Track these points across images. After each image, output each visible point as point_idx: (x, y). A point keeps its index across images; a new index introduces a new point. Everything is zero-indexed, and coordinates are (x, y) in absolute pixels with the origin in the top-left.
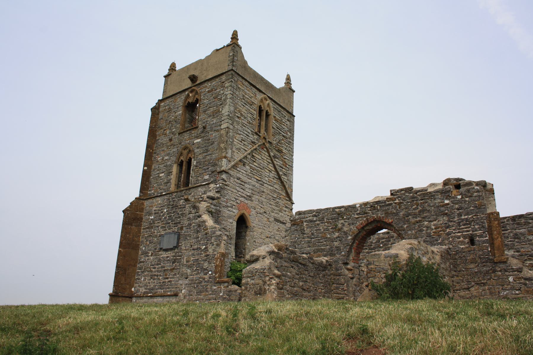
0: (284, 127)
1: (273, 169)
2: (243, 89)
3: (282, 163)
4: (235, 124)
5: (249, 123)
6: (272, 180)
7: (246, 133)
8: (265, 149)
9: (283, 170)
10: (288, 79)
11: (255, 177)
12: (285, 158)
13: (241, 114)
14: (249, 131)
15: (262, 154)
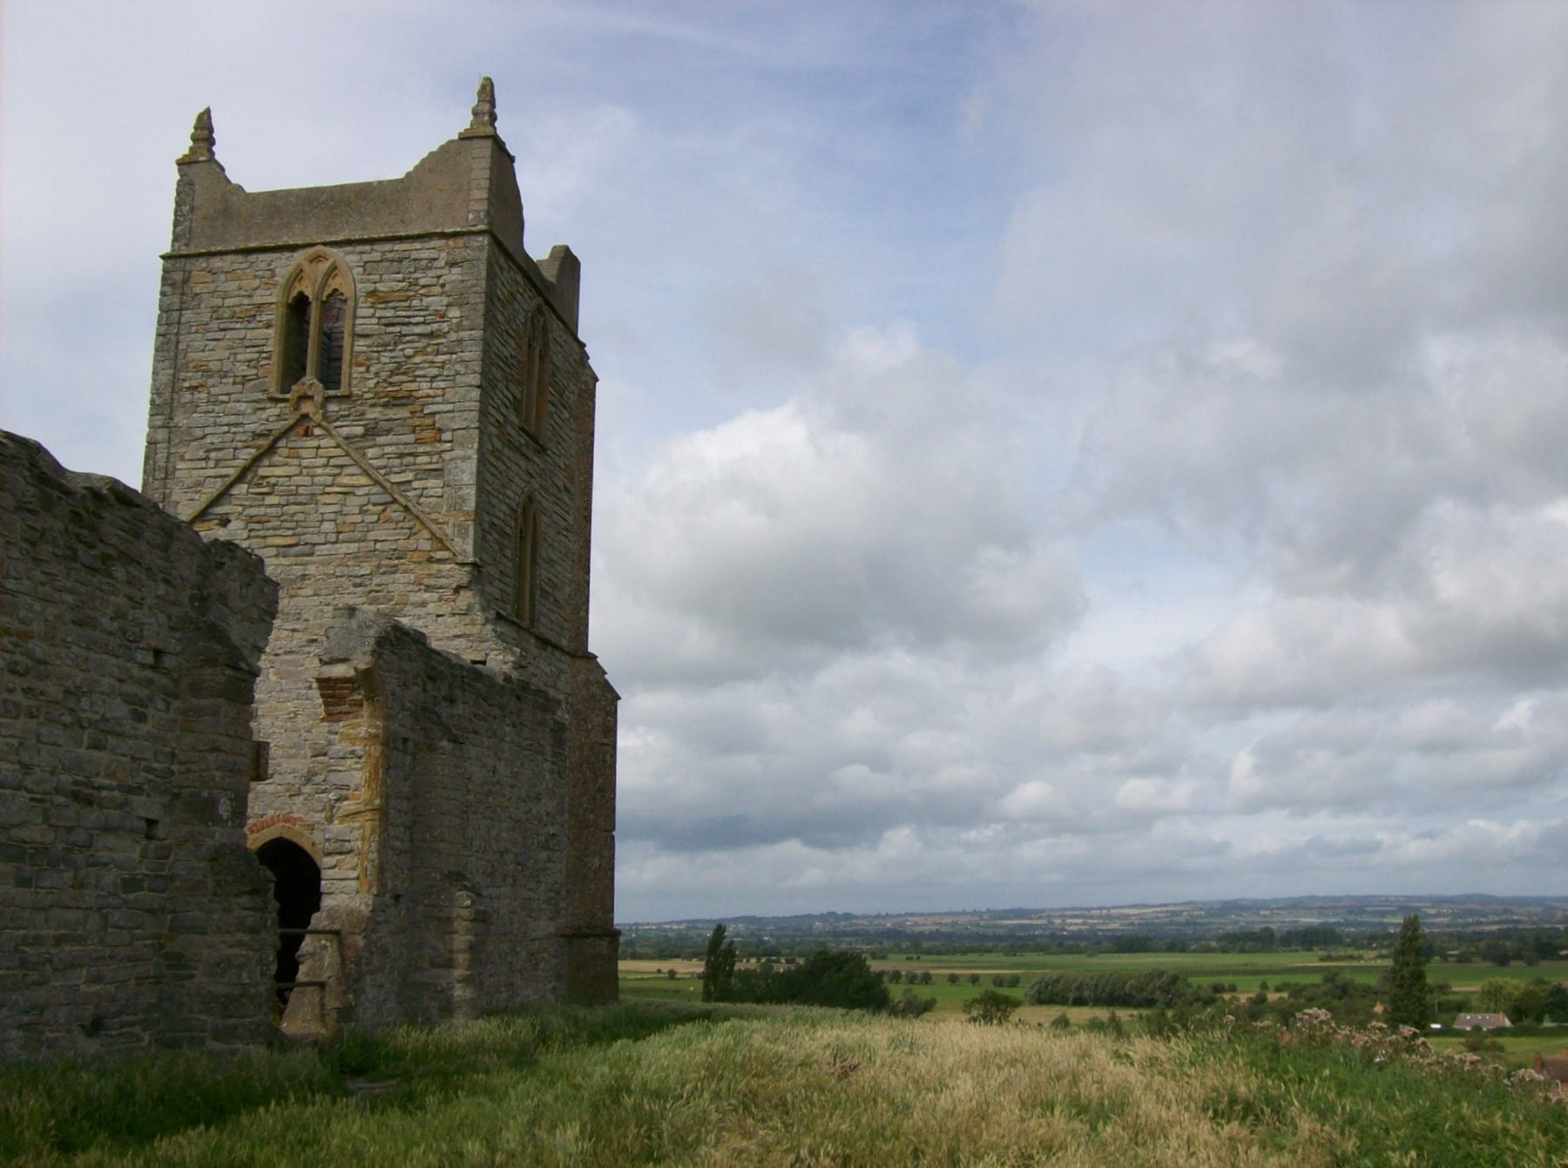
0: (427, 301)
1: (364, 480)
2: (212, 287)
3: (411, 438)
4: (181, 420)
5: (245, 379)
6: (358, 518)
7: (225, 420)
8: (317, 431)
9: (420, 460)
10: (487, 92)
11: (270, 541)
12: (433, 414)
13: (208, 373)
14: (243, 407)
15: (303, 453)
